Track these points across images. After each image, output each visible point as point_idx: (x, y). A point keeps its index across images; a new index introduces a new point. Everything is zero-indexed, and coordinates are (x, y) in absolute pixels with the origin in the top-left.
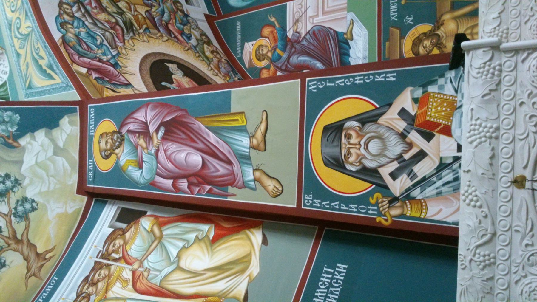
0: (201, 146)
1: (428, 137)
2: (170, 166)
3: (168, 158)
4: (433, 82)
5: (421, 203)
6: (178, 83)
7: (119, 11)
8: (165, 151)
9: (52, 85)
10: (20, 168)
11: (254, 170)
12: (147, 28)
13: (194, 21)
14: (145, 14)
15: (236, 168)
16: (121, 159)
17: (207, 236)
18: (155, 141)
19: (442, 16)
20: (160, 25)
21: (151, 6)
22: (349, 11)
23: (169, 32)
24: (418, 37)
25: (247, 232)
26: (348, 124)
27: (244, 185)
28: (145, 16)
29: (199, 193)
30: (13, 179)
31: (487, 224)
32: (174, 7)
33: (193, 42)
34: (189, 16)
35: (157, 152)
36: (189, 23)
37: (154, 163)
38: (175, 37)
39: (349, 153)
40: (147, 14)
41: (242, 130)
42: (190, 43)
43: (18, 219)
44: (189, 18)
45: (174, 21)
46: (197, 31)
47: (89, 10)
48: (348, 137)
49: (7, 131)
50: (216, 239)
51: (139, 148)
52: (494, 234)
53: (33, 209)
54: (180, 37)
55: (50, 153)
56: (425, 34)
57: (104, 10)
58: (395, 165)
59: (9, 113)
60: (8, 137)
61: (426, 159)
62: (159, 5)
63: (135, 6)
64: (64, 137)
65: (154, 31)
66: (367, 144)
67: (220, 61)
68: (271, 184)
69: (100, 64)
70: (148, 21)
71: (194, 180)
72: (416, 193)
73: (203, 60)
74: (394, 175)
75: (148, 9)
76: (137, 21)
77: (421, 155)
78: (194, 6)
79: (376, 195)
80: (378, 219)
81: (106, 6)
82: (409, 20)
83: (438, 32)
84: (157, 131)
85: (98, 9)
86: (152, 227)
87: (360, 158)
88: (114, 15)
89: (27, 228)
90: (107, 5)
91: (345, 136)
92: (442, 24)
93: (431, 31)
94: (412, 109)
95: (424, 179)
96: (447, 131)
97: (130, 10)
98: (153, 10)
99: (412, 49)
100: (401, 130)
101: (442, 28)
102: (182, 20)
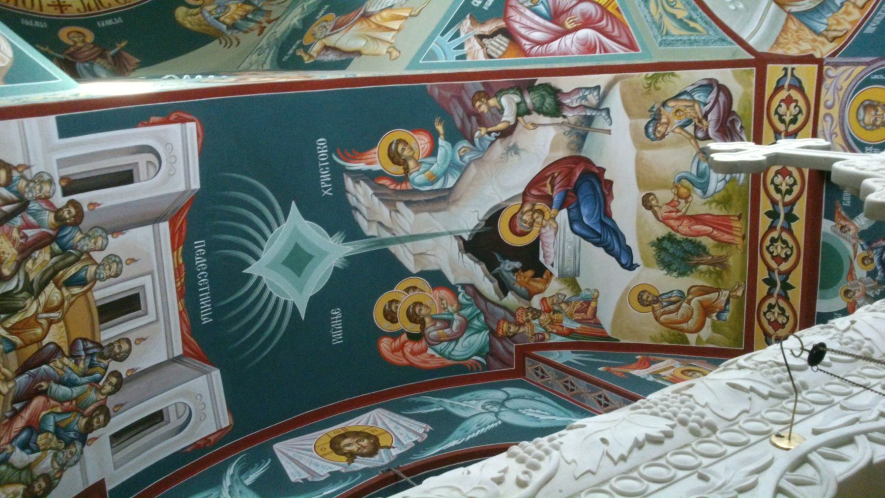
7: (35, 286)
12: (14, 347)
13: (75, 458)
14: (51, 343)
20: (33, 376)
21: (73, 356)
23: (26, 397)
28: (45, 342)
32: (91, 408)
33: (19, 457)
34: (83, 445)
36: (67, 446)
38: (16, 414)
40: (52, 346)
42: (13, 448)
44: (78, 446)
45: (59, 410)
46: (52, 466)
47: (12, 221)
54: (19, 423)
57: (27, 251)
62: (84, 375)
63: (59, 321)
70: (33, 348)
75: (66, 349)
76: (26, 324)
78: (113, 454)
81: (35, 259)
85: (22, 241)
90: (39, 261)
97: (47, 310)
98: (66, 360)
102: (67, 429)
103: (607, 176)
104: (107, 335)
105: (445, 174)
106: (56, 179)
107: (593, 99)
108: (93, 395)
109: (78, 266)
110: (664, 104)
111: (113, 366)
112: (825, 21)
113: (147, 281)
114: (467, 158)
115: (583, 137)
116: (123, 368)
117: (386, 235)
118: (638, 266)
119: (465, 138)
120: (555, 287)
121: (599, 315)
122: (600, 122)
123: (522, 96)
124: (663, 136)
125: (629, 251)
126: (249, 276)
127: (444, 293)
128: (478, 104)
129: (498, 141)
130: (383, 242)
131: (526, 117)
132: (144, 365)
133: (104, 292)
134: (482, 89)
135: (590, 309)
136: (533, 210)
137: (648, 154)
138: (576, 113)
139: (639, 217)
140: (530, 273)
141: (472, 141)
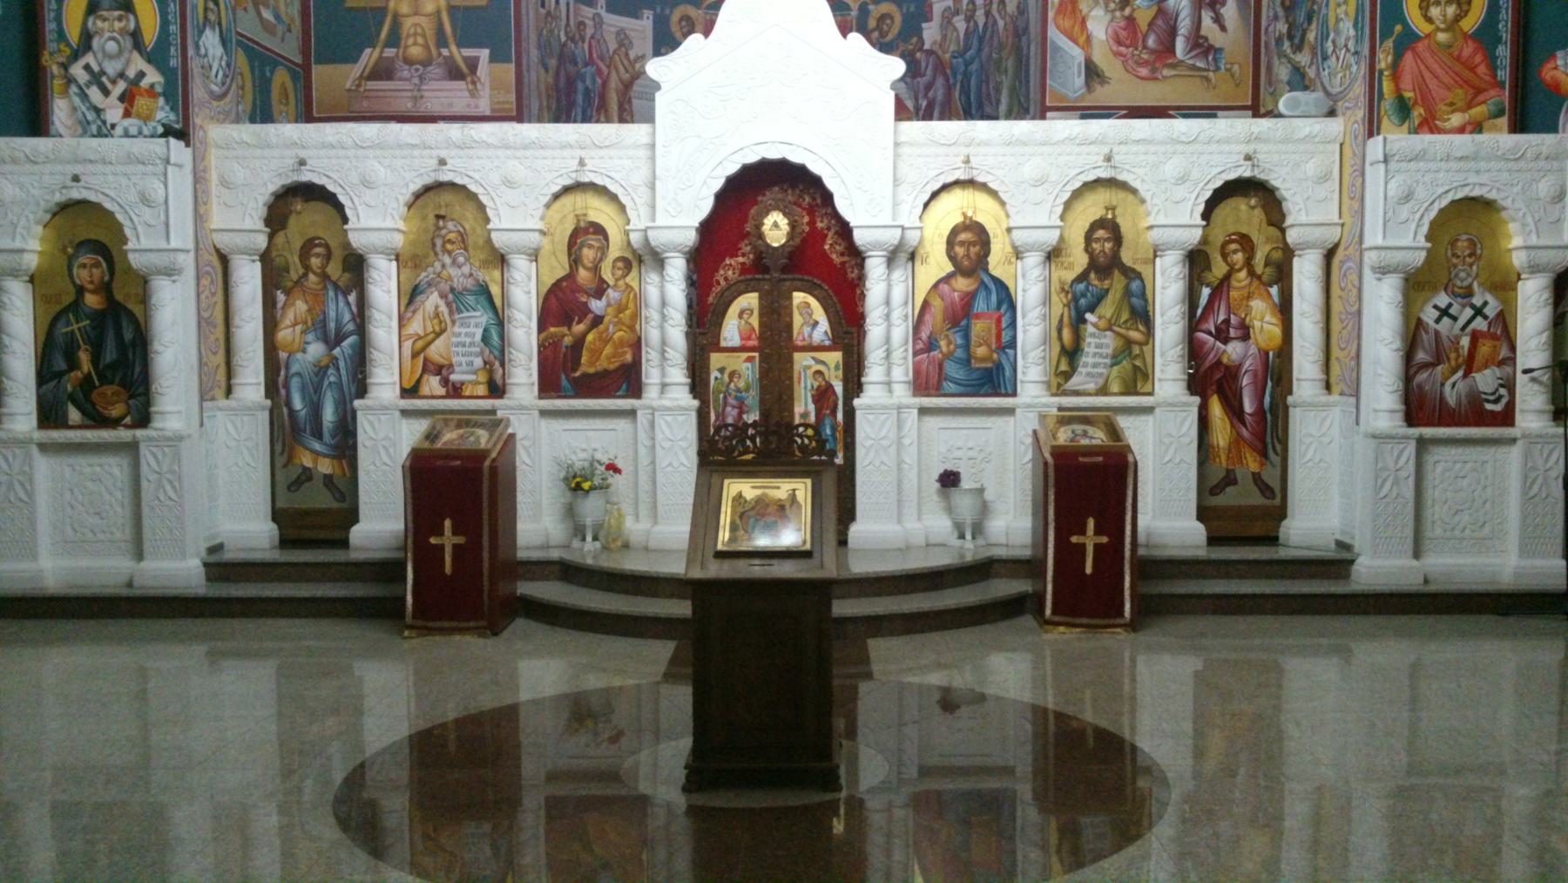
1: (122, 98)
4: (167, 101)
26: (132, 17)
39: (105, 20)
48: (120, 19)
58: (96, 68)
66: (113, 39)
72: (74, 89)
74: (87, 67)
77: (106, 92)
80: (46, 53)
87: (100, 32)
91: (121, 15)
94: (145, 83)
95: (86, 95)
96: (127, 114)
100: (127, 73)
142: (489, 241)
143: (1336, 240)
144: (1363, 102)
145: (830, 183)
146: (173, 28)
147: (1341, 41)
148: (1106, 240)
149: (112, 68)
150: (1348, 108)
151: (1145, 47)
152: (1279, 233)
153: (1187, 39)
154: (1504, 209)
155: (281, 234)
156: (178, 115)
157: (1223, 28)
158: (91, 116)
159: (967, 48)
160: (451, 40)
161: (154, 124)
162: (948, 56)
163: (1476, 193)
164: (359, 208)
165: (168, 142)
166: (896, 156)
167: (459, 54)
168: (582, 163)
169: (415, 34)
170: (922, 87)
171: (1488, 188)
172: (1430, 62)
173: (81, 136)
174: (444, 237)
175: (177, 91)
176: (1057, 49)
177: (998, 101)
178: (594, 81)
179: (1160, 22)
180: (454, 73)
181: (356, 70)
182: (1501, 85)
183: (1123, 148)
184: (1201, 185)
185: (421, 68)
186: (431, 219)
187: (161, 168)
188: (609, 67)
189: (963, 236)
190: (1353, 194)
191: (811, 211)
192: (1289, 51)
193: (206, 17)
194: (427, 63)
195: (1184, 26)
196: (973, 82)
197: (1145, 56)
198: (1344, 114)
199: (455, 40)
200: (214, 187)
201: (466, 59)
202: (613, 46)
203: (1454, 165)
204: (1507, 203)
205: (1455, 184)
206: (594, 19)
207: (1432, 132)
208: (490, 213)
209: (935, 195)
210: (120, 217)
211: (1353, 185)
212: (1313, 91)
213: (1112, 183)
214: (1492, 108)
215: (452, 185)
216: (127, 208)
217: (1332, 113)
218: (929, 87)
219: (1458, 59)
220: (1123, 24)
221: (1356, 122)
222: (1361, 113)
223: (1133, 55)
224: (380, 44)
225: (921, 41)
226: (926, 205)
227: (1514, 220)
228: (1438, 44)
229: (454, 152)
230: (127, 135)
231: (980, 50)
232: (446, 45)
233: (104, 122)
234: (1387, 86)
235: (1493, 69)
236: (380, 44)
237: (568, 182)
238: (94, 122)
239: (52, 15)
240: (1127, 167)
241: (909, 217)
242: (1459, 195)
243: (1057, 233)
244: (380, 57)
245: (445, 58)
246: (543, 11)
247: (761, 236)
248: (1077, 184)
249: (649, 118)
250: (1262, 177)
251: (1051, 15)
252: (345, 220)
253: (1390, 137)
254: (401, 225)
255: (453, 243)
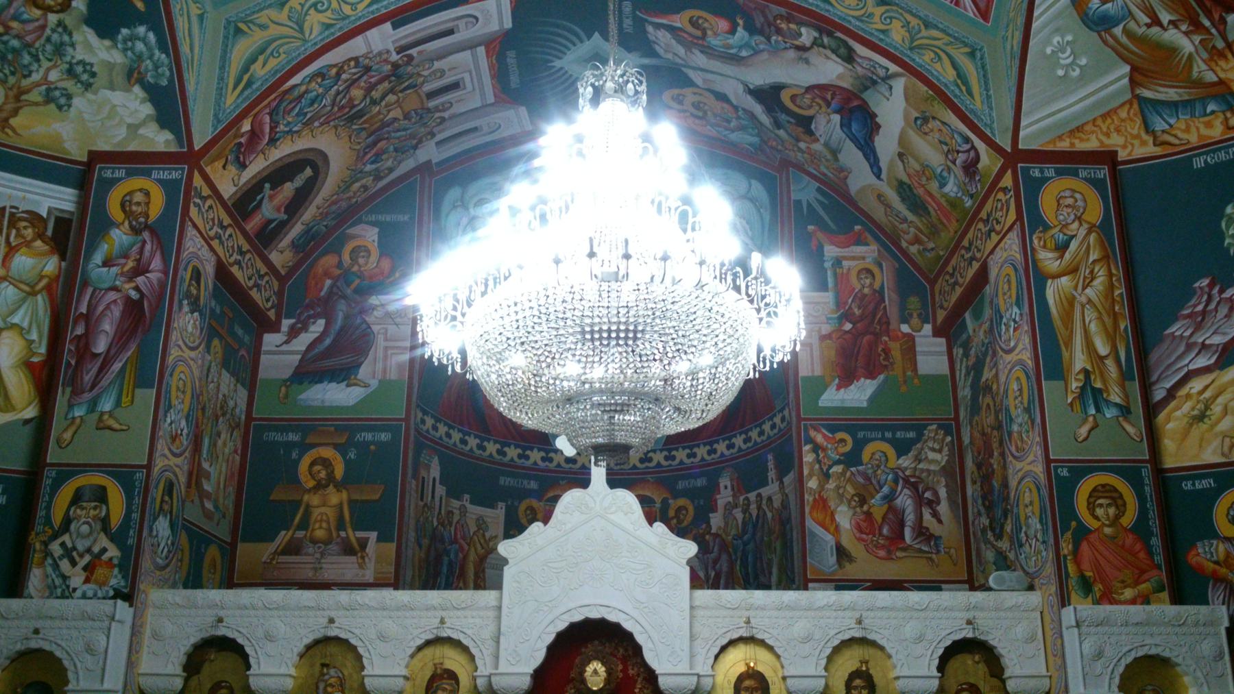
0: (113, 352)
1: (85, 569)
2: (101, 308)
3: (108, 307)
5: (41, 564)
6: (274, 195)
8: (115, 301)
9: (227, 85)
10: (105, 88)
11: (81, 417)
12: (364, 129)
15: (87, 396)
16: (117, 231)
17: (34, 354)
18: (127, 286)
19: (347, 490)
22: (380, 381)
24: (331, 464)
25: (36, 401)
26: (104, 508)
27: (71, 406)
29: (70, 350)
30: (91, 80)
31: (13, 615)
35: (115, 289)
37: (106, 285)
38: (366, 153)
41: (118, 403)
43: (44, 93)
48: (95, 508)
49: (147, 71)
50: (28, 365)
51: (123, 261)
52: (7, 619)
53: (60, 108)
55: (129, 121)
56: (333, 472)
58: (69, 545)
59: (168, 73)
60: (139, 73)
61: (71, 567)
64: (151, 135)
65: (364, 134)
66: (87, 523)
67: (350, 198)
68: (67, 436)
69: (267, 130)
71: (81, 345)
72: (49, 561)
73: (339, 187)
74: (63, 545)
75: (401, 118)
76: (372, 117)
77: (74, 563)
79: (50, 531)
80: (33, 533)
82: (352, 455)
83: (331, 486)
84: (137, 289)
86: (47, 276)
87: (78, 518)
88: (368, 100)
89: (37, 104)
92: (338, 491)
93: (334, 478)
94: (105, 557)
95: (58, 566)
96: (87, 581)
99: (321, 458)
101: (335, 490)
103: (877, 120)
104: (432, 104)
105: (740, 48)
106: (392, 49)
107: (882, 73)
108: (423, 130)
109: (411, 81)
110: (934, 118)
111: (437, 115)
112: (1172, 121)
113: (467, 76)
114: (762, 47)
115: (866, 88)
116: (446, 115)
117: (680, 61)
118: (882, 180)
119: (763, 35)
120: (817, 147)
121: (849, 181)
122: (883, 88)
123: (821, 35)
124: (926, 134)
125: (880, 170)
126: (554, 67)
127: (725, 105)
128: (778, 22)
129: (792, 50)
130: (677, 64)
131: (821, 49)
132: (463, 110)
133: (428, 88)
134: (784, 14)
135: (842, 175)
136: (813, 100)
137: (911, 133)
138: (865, 71)
139: (892, 161)
140: (800, 129)
141: (768, 39)
142: (363, 684)
143: (1047, 689)
144: (1054, 579)
145: (640, 638)
146: (134, 515)
147: (1031, 532)
148: (863, 688)
149: (81, 545)
150: (1042, 584)
151: (881, 534)
152: (1000, 684)
153: (913, 529)
154: (1179, 665)
155: (195, 678)
156: (127, 581)
157: (940, 521)
158: (58, 582)
159: (744, 532)
160: (348, 525)
161: (106, 588)
162: (730, 538)
163: (1153, 651)
164: (261, 657)
165: (115, 603)
166: (692, 617)
167: (353, 535)
168: (442, 621)
169: (321, 521)
170: (710, 561)
171: (1163, 648)
172: (1101, 548)
173: (48, 597)
174: (326, 681)
175: (130, 565)
176: (813, 534)
177: (770, 573)
178: (457, 555)
179: (891, 516)
180: (348, 550)
181: (272, 547)
182: (1158, 567)
183: (872, 614)
184: (934, 644)
185: (323, 546)
186: (317, 668)
187: (107, 623)
188: (469, 545)
189: (747, 683)
190: (1056, 653)
191: (624, 660)
192: (992, 539)
193: (161, 508)
194: (327, 542)
195: (910, 518)
196: (750, 559)
197: (882, 542)
198: (1041, 589)
199: (352, 524)
200: (146, 638)
201: (358, 539)
202: (473, 529)
203: (1133, 630)
204: (1179, 660)
205: (1136, 645)
206: (460, 509)
207: (1111, 603)
208: (365, 661)
209: (723, 649)
210: (66, 663)
211: (1055, 645)
212: (1014, 570)
213: (863, 641)
214: (1155, 585)
215: (337, 639)
216: (73, 655)
217: (1031, 588)
218: (715, 562)
219: (1123, 547)
220: (862, 517)
221: (1050, 595)
222: (1053, 589)
223: (872, 541)
224: (293, 528)
225: (709, 526)
226: (717, 657)
227: (1187, 674)
228: (1106, 535)
229: (342, 612)
230: (84, 596)
231: (754, 534)
232: (345, 530)
233: (68, 587)
234: (1071, 568)
235: (1150, 554)
236: (293, 528)
237: (430, 636)
238: (60, 587)
239: (44, 504)
240: (875, 628)
241: (703, 667)
242: (1140, 654)
243: (823, 682)
244: (292, 537)
245: (342, 538)
246: (422, 504)
247: (583, 681)
248: (836, 642)
249: (498, 586)
250: (982, 638)
251: (807, 510)
252: (248, 667)
253: (1079, 607)
254: (293, 671)
255: (334, 686)
